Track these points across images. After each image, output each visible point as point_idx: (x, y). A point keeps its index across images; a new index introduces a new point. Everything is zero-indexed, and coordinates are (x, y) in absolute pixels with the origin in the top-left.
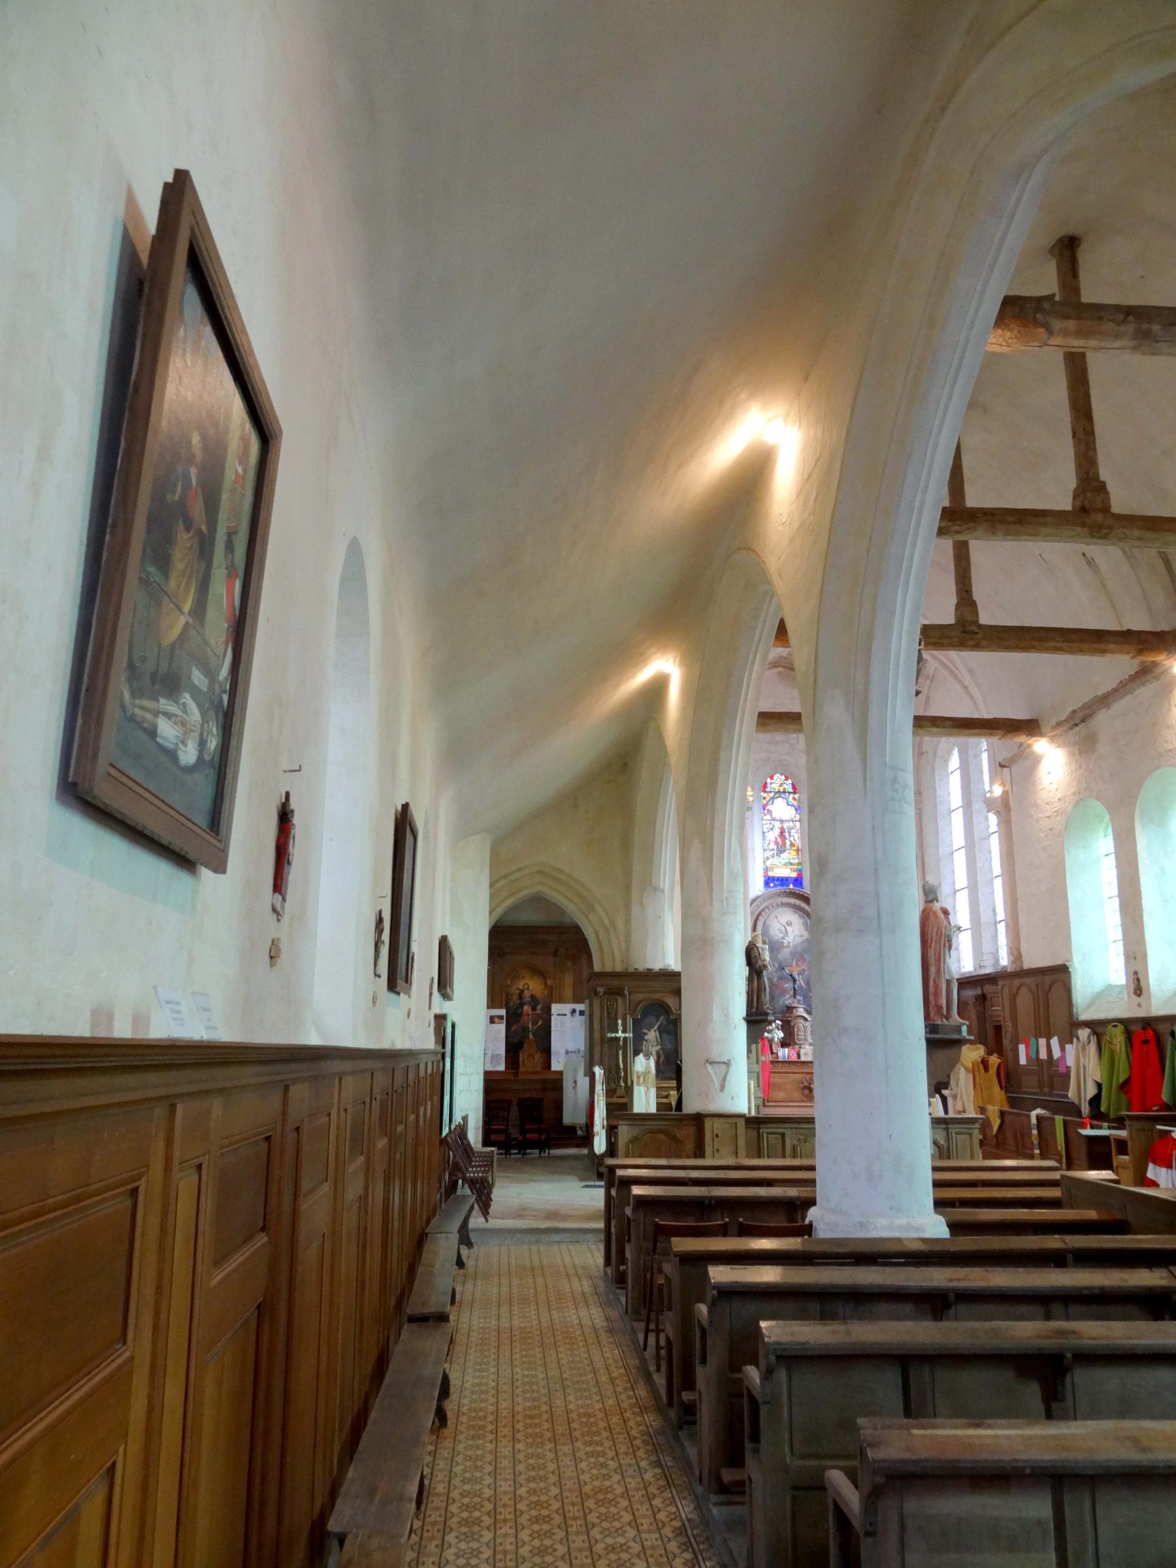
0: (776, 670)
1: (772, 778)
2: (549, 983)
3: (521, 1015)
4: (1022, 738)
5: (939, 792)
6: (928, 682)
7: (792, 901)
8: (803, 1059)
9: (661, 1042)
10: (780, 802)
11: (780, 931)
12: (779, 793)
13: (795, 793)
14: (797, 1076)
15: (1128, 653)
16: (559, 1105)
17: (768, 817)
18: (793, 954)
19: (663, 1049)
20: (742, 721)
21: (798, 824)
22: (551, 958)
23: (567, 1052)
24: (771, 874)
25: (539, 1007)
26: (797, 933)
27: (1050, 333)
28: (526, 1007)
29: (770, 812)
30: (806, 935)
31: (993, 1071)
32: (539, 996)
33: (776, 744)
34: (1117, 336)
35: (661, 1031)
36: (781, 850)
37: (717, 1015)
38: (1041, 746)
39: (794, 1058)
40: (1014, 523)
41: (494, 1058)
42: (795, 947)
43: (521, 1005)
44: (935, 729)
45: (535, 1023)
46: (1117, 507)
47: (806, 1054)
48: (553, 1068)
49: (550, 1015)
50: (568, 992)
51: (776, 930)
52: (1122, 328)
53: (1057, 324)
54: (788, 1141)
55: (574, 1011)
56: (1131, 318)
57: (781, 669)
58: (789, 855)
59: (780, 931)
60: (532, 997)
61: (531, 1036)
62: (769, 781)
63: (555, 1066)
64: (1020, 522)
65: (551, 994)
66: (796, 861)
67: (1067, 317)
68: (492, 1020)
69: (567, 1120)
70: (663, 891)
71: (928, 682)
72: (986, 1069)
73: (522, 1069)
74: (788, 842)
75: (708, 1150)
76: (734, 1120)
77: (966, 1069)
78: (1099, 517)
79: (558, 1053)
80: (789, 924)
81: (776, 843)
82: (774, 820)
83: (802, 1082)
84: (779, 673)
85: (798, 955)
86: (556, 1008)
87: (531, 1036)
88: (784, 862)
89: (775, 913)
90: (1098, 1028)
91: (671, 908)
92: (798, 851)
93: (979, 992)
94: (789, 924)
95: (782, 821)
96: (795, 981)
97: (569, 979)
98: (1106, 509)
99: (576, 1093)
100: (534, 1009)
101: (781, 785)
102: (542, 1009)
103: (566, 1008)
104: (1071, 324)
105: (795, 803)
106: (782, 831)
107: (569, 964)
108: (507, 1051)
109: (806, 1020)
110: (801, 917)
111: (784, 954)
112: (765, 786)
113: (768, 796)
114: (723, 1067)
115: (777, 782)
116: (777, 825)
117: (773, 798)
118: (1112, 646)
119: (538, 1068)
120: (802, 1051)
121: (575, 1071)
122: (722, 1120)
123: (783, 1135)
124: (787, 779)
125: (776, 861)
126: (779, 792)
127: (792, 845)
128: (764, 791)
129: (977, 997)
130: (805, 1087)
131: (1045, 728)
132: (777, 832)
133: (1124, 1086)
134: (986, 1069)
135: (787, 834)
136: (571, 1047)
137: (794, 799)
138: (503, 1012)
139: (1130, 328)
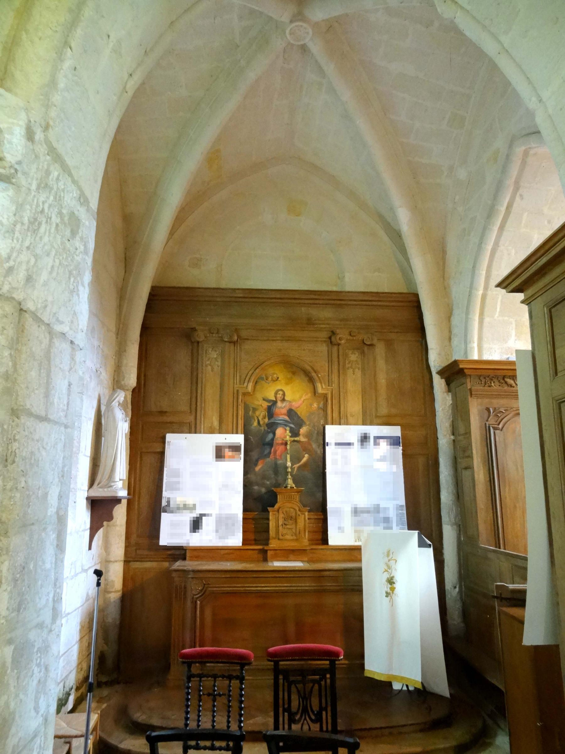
2: (320, 390)
3: (271, 444)
16: (353, 626)
22: (323, 348)
23: (356, 511)
25: (303, 430)
28: (279, 431)
32: (302, 412)
41: (223, 522)
43: (272, 427)
45: (296, 459)
48: (332, 541)
49: (324, 445)
50: (354, 405)
55: (364, 439)
60: (291, 413)
61: (290, 482)
63: (335, 538)
65: (325, 409)
68: (220, 453)
69: (375, 664)
73: (273, 544)
79: (338, 512)
86: (333, 433)
87: (290, 482)
97: (353, 383)
99: (392, 604)
100: (294, 433)
102: (309, 435)
103: (352, 432)
107: (354, 357)
108: (246, 509)
119: (305, 542)
121: (390, 556)
136: (363, 501)
138: (239, 439)
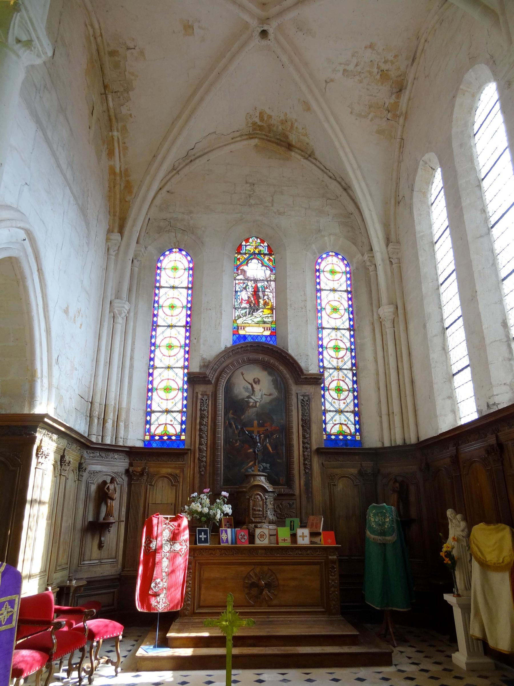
0: (254, 142)
1: (247, 240)
5: (418, 228)
6: (401, 120)
7: (260, 357)
8: (258, 542)
11: (246, 389)
12: (254, 255)
13: (270, 254)
14: (242, 568)
17: (241, 277)
18: (259, 416)
21: (273, 284)
24: (241, 332)
26: (265, 391)
29: (244, 272)
30: (275, 394)
33: (250, 206)
36: (254, 306)
39: (244, 542)
42: (263, 407)
47: (262, 536)
51: (241, 389)
57: (257, 140)
58: (263, 314)
59: (246, 389)
62: (244, 243)
66: (270, 320)
71: (401, 120)
74: (261, 301)
77: (485, 566)
80: (257, 381)
81: (249, 302)
82: (248, 279)
83: (248, 576)
84: (256, 146)
85: (265, 416)
88: (256, 320)
92: (272, 309)
93: (492, 440)
94: (257, 381)
95: (256, 281)
101: (256, 248)
105: (271, 264)
106: (256, 291)
109: (265, 490)
110: (270, 374)
111: (251, 413)
112: (240, 247)
117: (247, 261)
120: (258, 531)
124: (262, 241)
125: (249, 319)
126: (254, 253)
127: (266, 304)
128: (239, 253)
129: (490, 450)
130: (253, 585)
132: (250, 290)
135: (261, 294)
137: (270, 260)
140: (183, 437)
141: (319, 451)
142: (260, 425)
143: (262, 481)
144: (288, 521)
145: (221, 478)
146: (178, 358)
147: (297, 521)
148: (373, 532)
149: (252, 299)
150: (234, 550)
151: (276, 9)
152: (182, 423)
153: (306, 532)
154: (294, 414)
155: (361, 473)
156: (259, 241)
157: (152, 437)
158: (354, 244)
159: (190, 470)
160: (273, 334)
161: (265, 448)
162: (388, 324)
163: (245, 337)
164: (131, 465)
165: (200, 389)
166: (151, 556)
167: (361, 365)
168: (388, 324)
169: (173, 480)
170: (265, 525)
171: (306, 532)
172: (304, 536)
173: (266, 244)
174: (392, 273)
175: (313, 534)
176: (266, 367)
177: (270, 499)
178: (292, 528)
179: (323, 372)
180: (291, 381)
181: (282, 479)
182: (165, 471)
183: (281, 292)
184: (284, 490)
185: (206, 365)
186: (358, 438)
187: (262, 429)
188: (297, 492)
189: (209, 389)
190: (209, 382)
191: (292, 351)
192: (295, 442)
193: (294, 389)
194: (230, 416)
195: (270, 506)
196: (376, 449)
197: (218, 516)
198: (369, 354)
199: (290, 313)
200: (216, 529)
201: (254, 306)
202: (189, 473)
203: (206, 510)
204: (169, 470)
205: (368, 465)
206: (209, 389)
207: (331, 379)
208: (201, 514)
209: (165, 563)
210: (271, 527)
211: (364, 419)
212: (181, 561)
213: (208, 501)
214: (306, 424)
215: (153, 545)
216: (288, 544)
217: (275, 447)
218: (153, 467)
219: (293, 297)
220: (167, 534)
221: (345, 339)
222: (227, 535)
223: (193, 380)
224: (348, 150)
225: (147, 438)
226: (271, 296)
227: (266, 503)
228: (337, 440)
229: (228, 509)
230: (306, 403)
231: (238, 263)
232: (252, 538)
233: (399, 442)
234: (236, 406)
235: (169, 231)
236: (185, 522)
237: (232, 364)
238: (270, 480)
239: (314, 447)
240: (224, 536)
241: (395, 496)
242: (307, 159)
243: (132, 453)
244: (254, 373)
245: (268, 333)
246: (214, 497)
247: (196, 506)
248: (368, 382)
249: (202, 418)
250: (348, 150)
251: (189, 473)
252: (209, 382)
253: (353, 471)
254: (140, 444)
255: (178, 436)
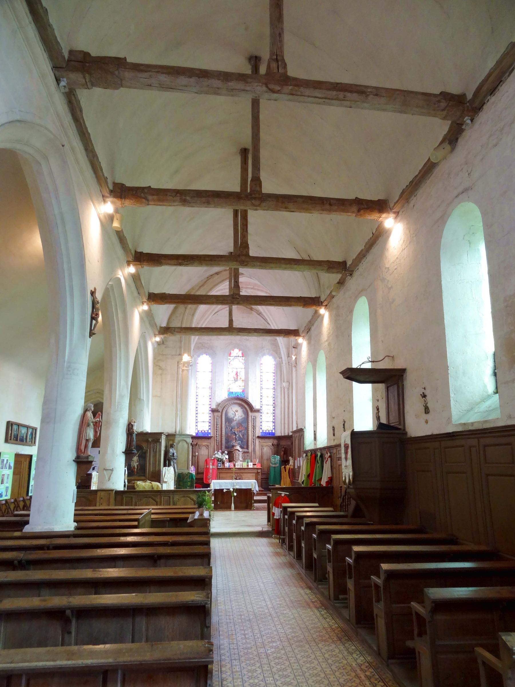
1: (233, 350)
4: (292, 338)
7: (238, 402)
8: (236, 467)
9: (139, 461)
10: (236, 360)
11: (233, 414)
15: (300, 306)
19: (139, 464)
20: (119, 336)
24: (231, 391)
26: (240, 415)
27: (148, 200)
30: (243, 416)
31: (287, 471)
34: (174, 201)
35: (139, 457)
36: (236, 380)
37: (109, 451)
38: (300, 340)
40: (209, 261)
42: (239, 421)
44: (255, 334)
46: (252, 254)
51: (231, 414)
52: (175, 198)
53: (150, 197)
54: (134, 500)
56: (178, 195)
59: (233, 414)
64: (211, 260)
67: (153, 195)
70: (143, 400)
72: (285, 471)
74: (239, 377)
75: (98, 504)
76: (110, 492)
78: (243, 258)
80: (237, 411)
85: (239, 424)
89: (230, 408)
90: (306, 452)
91: (148, 406)
94: (237, 411)
96: (236, 435)
98: (247, 255)
104: (155, 197)
110: (242, 408)
111: (234, 423)
112: (230, 354)
113: (231, 358)
114: (110, 471)
115: (236, 352)
116: (235, 371)
118: (293, 303)
120: (236, 464)
122: (104, 492)
123: (132, 497)
124: (240, 350)
131: (301, 334)
133: (309, 476)
134: (285, 471)
135: (238, 374)
139: (178, 198)
140: (210, 431)
141: (258, 437)
142: (238, 428)
143: (238, 448)
144: (246, 461)
145: (223, 447)
146: (207, 401)
147: (249, 461)
148: (272, 463)
149: (235, 376)
150: (229, 469)
151: (245, 286)
152: (209, 426)
153: (252, 464)
154: (250, 424)
155: (273, 445)
156: (238, 350)
157: (198, 431)
158: (277, 353)
159: (212, 443)
160: (243, 391)
161: (239, 436)
162: (286, 390)
163: (232, 393)
164: (193, 441)
165: (216, 414)
166: (207, 469)
167: (276, 403)
168: (286, 390)
169: (207, 447)
170: (239, 462)
171: (252, 464)
172: (251, 465)
173: (241, 352)
174: (289, 367)
175: (253, 465)
176: (240, 405)
177: (241, 453)
178: (248, 463)
179: (261, 407)
180: (249, 411)
181: (245, 447)
182: (204, 444)
183: (247, 374)
184: (246, 450)
185: (218, 405)
186: (274, 431)
187: (238, 429)
188: (250, 451)
189: (219, 414)
190: (219, 412)
191: (251, 400)
192: (250, 434)
193: (250, 414)
194: (227, 424)
195: (241, 456)
196: (279, 436)
197: (224, 459)
198: (279, 400)
199: (250, 383)
200: (223, 463)
201: (236, 380)
202: (212, 445)
203: (220, 457)
204: (206, 444)
205: (275, 442)
206: (219, 414)
207: (264, 410)
208: (219, 459)
209: (211, 471)
210: (241, 462)
211: (276, 425)
212: (215, 471)
213: (220, 454)
214: (254, 427)
215: (208, 466)
216: (246, 467)
217: (243, 436)
218: (200, 442)
219: (251, 377)
220: (211, 464)
221: (271, 393)
222: (227, 465)
223: (213, 411)
224: (273, 321)
225: (197, 432)
226: (242, 375)
227: (239, 454)
228: (265, 433)
229: (227, 457)
230: (254, 420)
231: (229, 361)
232: (235, 465)
233: (286, 434)
234: (229, 420)
235: (202, 349)
236: (216, 460)
237: (227, 404)
238: (242, 447)
239: (257, 436)
240: (226, 465)
241: (282, 453)
242: (259, 314)
243: (193, 438)
244: (236, 408)
245: (241, 391)
246: (223, 453)
247: (217, 456)
248: (278, 411)
249: (217, 425)
250: (273, 321)
251: (212, 445)
252: (219, 412)
253: (271, 444)
254: (194, 434)
255: (208, 431)
